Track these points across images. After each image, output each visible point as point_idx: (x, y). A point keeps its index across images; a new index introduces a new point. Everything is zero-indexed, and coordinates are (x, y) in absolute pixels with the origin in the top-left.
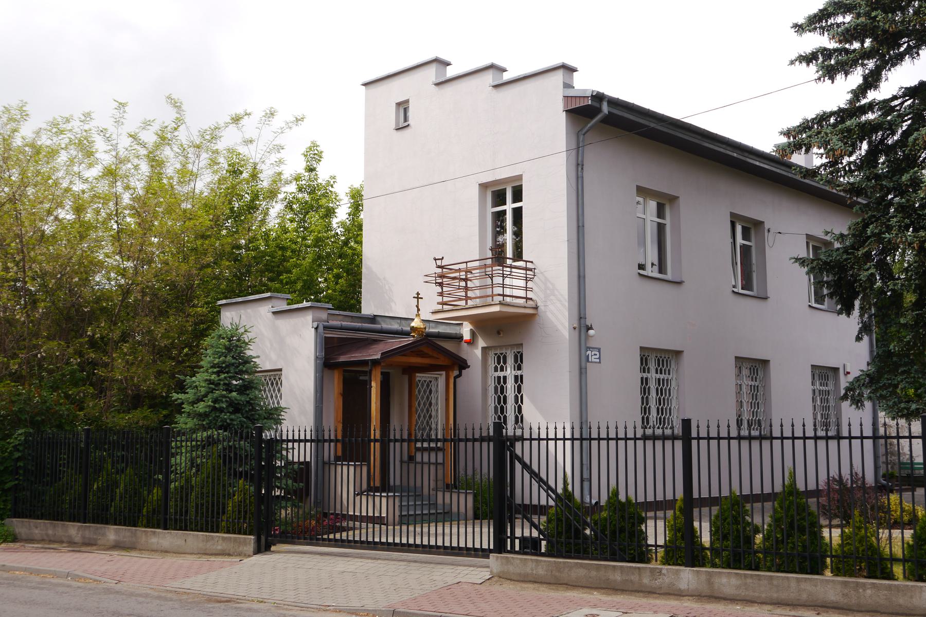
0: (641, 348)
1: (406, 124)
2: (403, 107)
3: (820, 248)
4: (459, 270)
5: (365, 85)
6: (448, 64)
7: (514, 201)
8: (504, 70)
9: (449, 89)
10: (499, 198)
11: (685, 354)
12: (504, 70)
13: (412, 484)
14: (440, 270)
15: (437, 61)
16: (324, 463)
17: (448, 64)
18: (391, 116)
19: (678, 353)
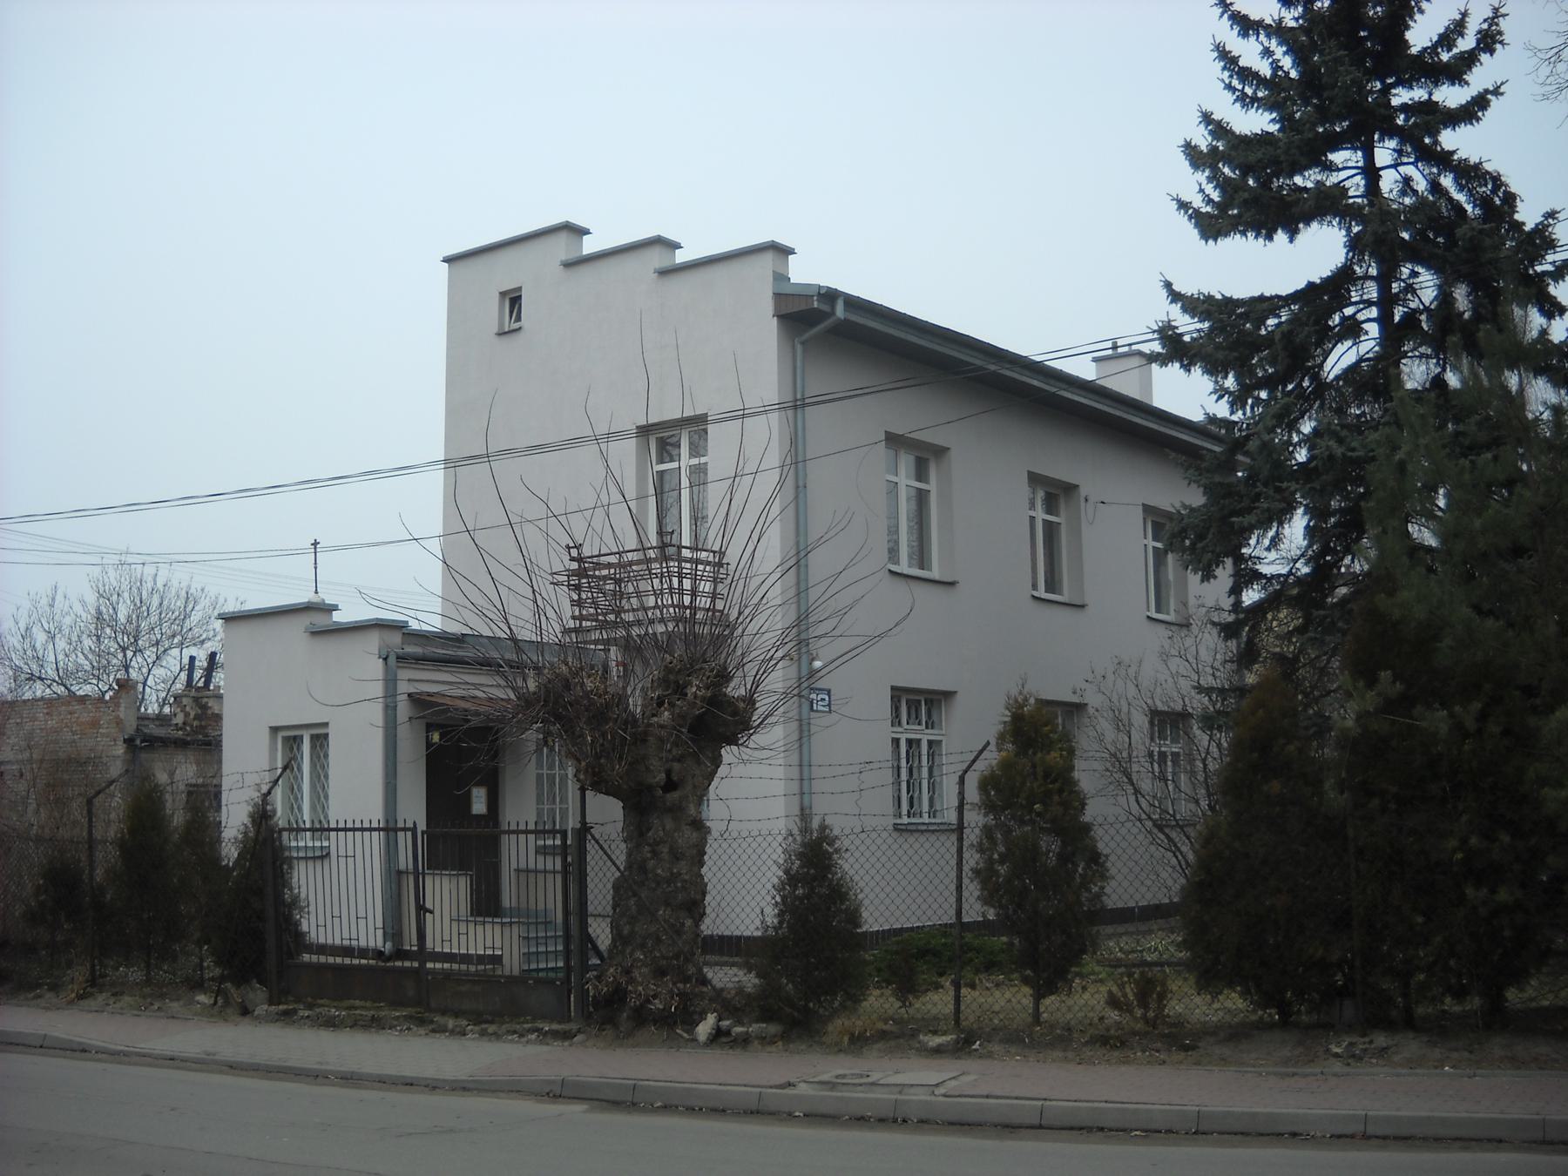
0: (893, 688)
1: (516, 326)
2: (513, 300)
3: (1163, 525)
4: (609, 565)
5: (448, 260)
6: (587, 232)
7: (691, 456)
8: (677, 246)
9: (676, 283)
10: (667, 449)
11: (958, 696)
12: (677, 246)
13: (541, 906)
14: (575, 565)
15: (658, 241)
16: (400, 873)
17: (587, 232)
18: (492, 312)
19: (948, 695)
